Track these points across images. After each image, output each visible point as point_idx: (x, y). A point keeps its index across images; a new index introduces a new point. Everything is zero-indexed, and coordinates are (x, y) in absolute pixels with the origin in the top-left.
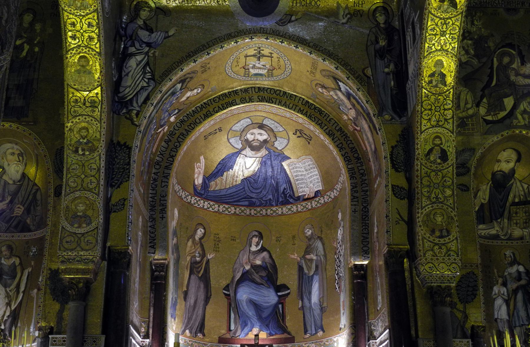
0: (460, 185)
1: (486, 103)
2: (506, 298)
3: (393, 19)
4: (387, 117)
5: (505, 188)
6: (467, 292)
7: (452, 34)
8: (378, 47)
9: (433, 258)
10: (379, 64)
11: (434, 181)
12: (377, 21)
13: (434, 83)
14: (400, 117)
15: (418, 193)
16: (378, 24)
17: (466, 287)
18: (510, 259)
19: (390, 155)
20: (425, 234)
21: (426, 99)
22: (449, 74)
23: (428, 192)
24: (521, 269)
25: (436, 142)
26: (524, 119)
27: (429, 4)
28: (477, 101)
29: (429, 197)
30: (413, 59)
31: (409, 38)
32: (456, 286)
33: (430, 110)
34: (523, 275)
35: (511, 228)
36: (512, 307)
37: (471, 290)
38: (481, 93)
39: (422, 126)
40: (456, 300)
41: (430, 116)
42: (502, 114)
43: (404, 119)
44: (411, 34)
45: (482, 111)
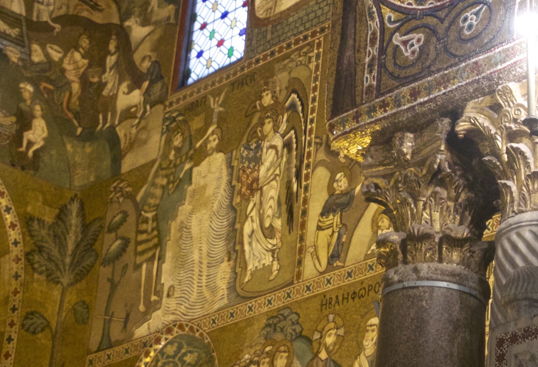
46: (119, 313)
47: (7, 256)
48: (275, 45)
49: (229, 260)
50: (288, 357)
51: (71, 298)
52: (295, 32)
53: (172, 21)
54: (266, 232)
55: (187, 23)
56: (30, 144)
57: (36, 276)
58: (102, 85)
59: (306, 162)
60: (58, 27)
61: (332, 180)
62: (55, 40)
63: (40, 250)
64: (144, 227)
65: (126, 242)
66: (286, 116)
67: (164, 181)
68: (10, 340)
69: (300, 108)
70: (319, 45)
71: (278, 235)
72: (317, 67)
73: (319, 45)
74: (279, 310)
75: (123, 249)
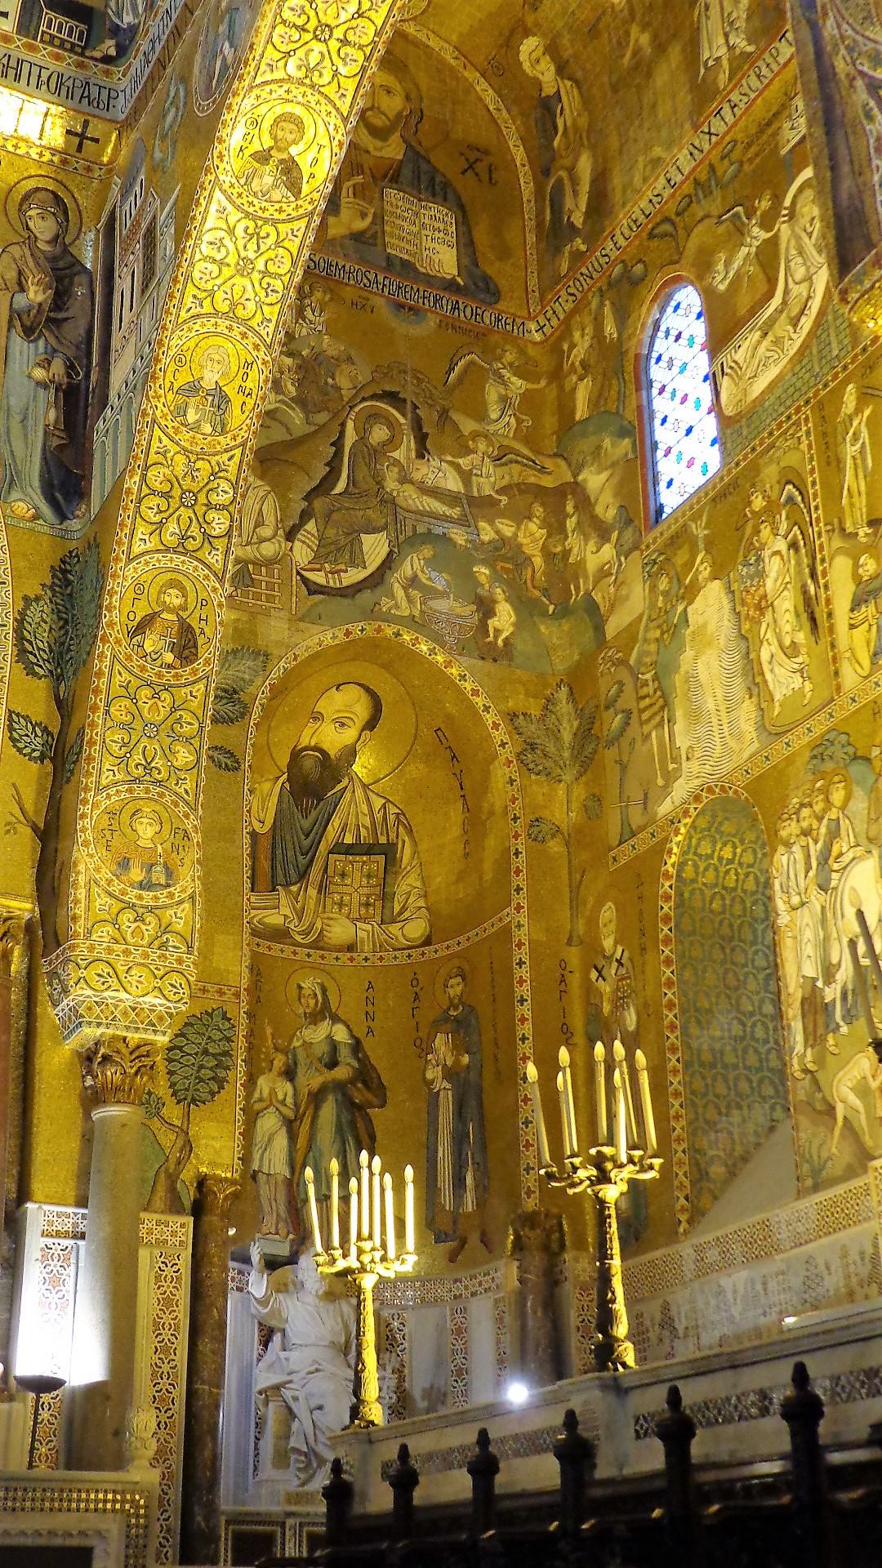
0: (216, 748)
1: (313, 535)
2: (290, 1114)
3: (77, 238)
4: (21, 508)
5: (320, 800)
6: (198, 1071)
7: (270, 275)
8: (21, 301)
9: (115, 947)
10: (18, 348)
11: (145, 713)
12: (28, 229)
13: (192, 416)
14: (62, 516)
15: (92, 743)
16: (32, 239)
17: (196, 1054)
18: (312, 1002)
19: (15, 620)
20: (97, 870)
21: (160, 458)
22: (241, 398)
23: (125, 745)
24: (341, 1034)
25: (167, 599)
26: (410, 600)
27: (221, 157)
28: (291, 523)
29: (123, 760)
30: (133, 339)
31: (122, 284)
32: (170, 1049)
33: (167, 495)
34: (345, 1055)
35: (326, 915)
36: (302, 1142)
37: (211, 1064)
38: (304, 504)
39: (136, 539)
40: (162, 1089)
41: (165, 515)
42: (353, 576)
43: (74, 524)
44: (138, 268)
45: (302, 553)
46: (634, 792)
47: (496, 762)
48: (755, 439)
49: (750, 698)
50: (845, 788)
51: (580, 792)
52: (774, 416)
53: (630, 456)
54: (788, 651)
55: (649, 454)
56: (497, 632)
57: (533, 777)
58: (566, 553)
59: (819, 556)
60: (504, 499)
61: (856, 566)
62: (502, 515)
63: (533, 747)
64: (644, 691)
65: (628, 713)
66: (784, 513)
67: (658, 633)
68: (517, 853)
69: (799, 499)
70: (807, 420)
71: (803, 650)
72: (810, 447)
73: (807, 420)
74: (823, 736)
75: (626, 723)
